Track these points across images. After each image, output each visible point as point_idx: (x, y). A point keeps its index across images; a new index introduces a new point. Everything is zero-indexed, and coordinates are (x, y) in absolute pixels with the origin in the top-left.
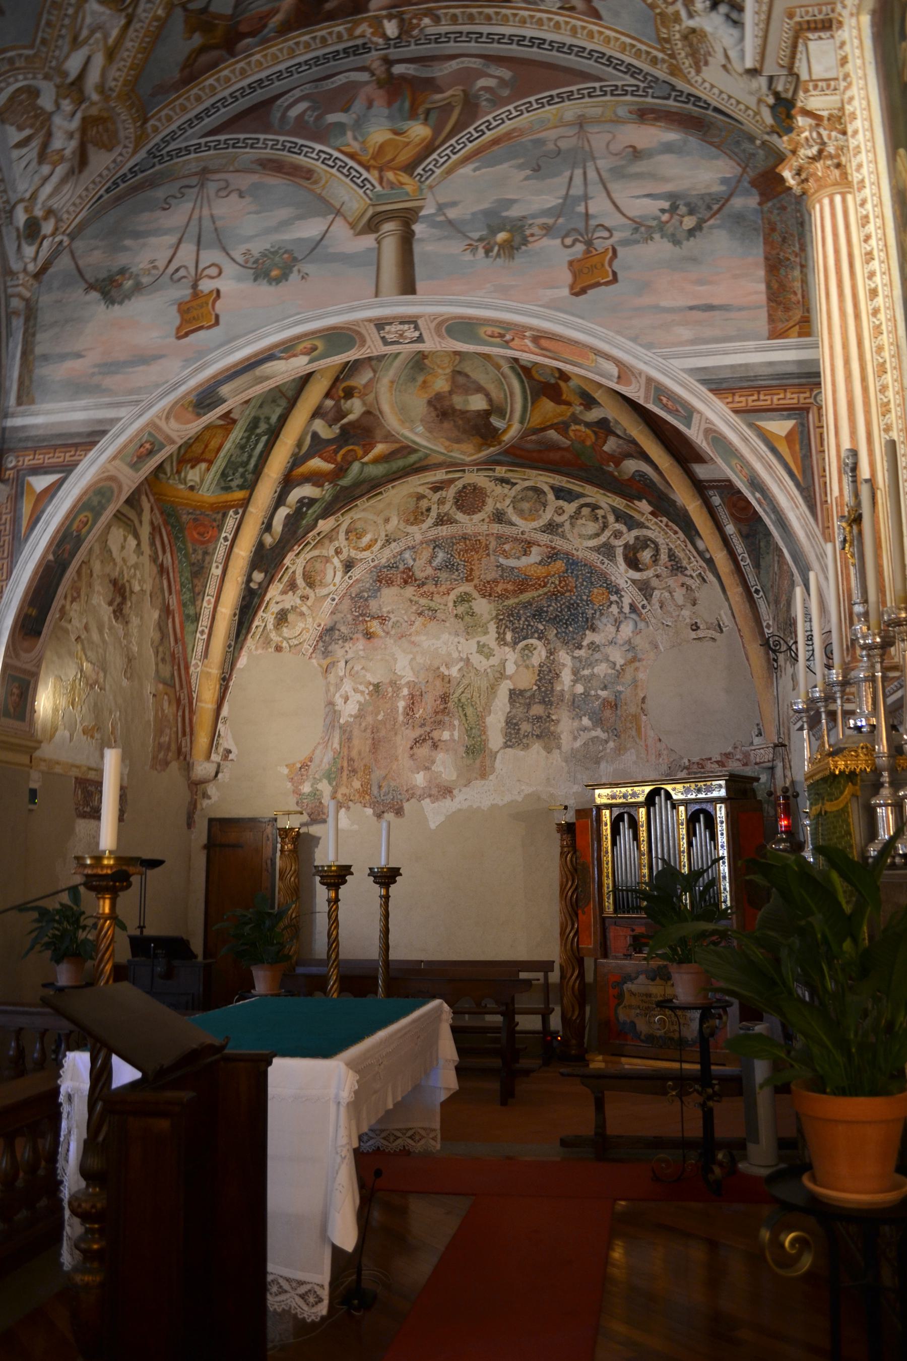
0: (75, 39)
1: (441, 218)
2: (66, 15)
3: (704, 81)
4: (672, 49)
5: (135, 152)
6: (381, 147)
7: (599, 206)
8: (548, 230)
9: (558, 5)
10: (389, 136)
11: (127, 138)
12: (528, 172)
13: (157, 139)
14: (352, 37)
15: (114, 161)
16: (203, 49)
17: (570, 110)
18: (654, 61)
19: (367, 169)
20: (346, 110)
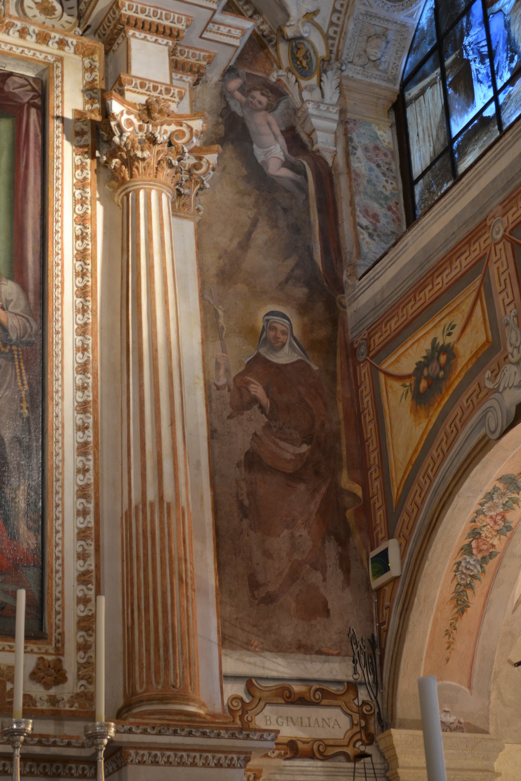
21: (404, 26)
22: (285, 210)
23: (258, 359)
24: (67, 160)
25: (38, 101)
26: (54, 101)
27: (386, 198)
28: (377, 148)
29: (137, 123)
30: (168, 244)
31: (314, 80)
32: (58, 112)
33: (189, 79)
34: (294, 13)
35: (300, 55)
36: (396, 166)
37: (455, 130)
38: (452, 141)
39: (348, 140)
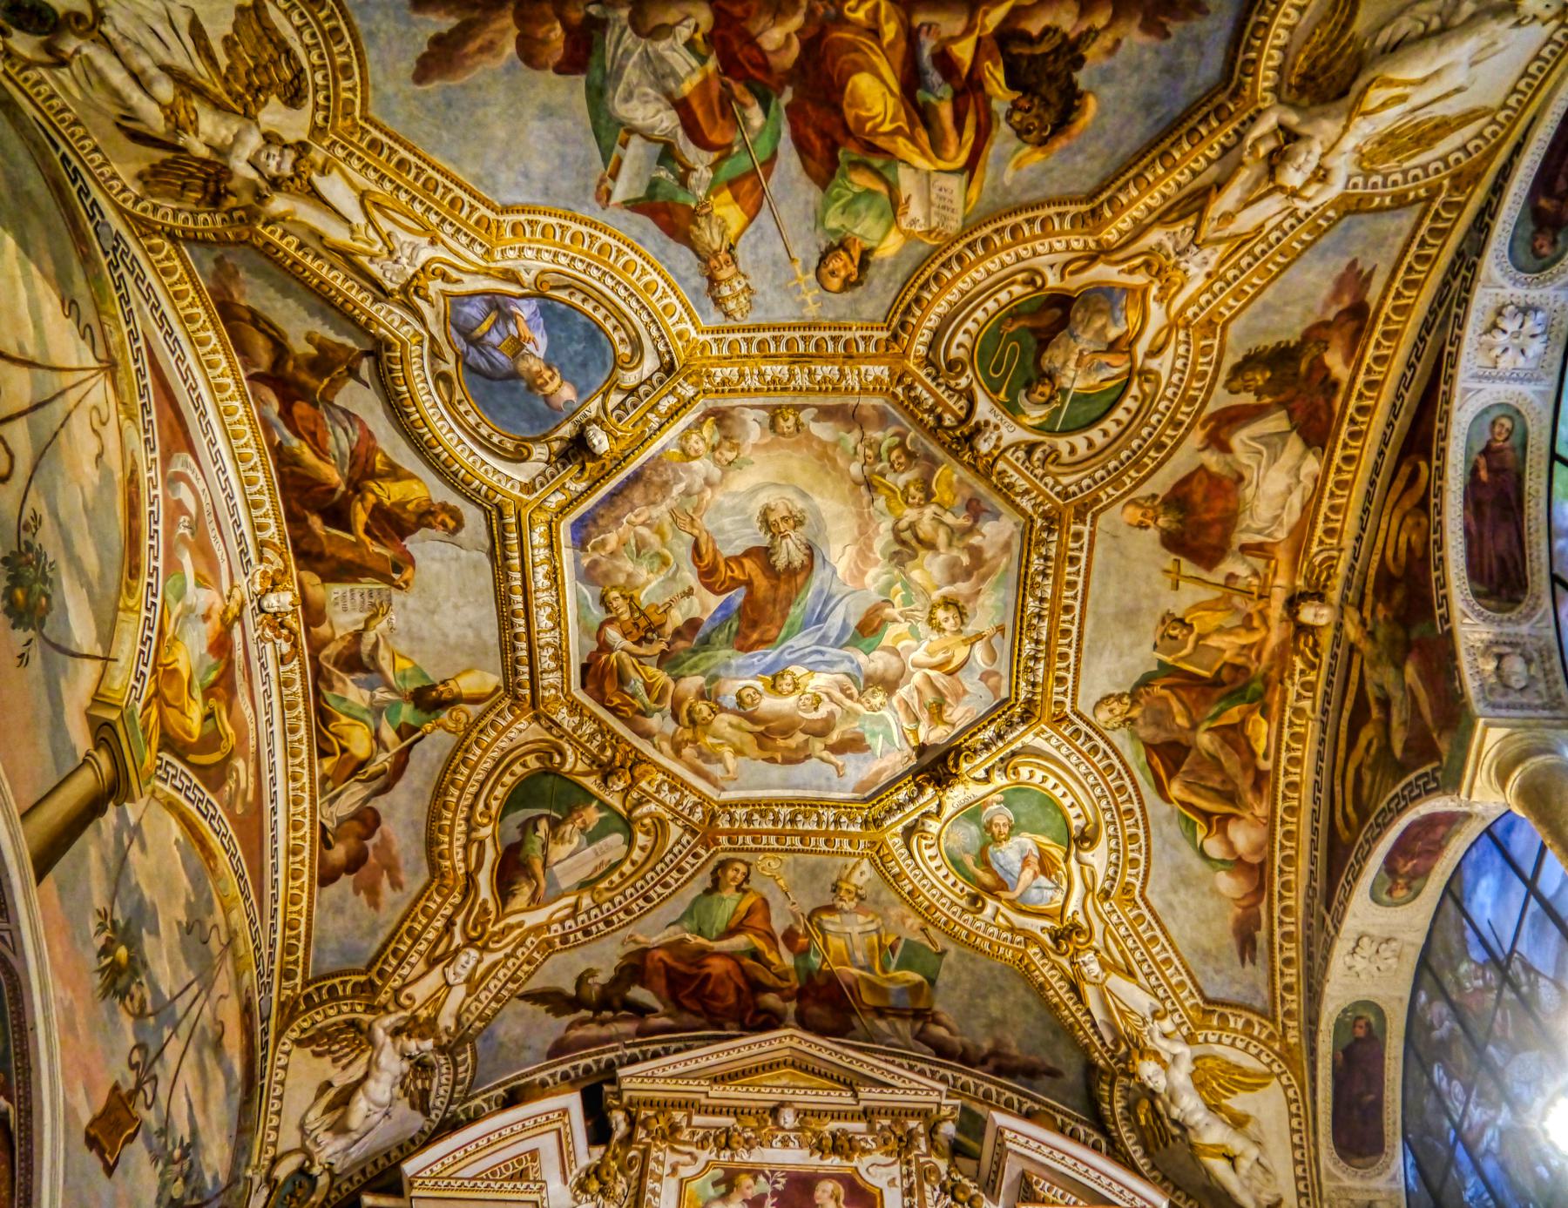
0: (377, 205)
1: (126, 841)
2: (414, 198)
3: (288, 1053)
4: (322, 1003)
5: (121, 211)
6: (175, 671)
7: (172, 1053)
8: (140, 1015)
9: (329, 825)
10: (186, 677)
11: (156, 209)
12: (184, 919)
13: (135, 249)
14: (261, 545)
15: (114, 176)
16: (279, 347)
17: (238, 918)
18: (287, 975)
19: (154, 671)
20: (198, 585)
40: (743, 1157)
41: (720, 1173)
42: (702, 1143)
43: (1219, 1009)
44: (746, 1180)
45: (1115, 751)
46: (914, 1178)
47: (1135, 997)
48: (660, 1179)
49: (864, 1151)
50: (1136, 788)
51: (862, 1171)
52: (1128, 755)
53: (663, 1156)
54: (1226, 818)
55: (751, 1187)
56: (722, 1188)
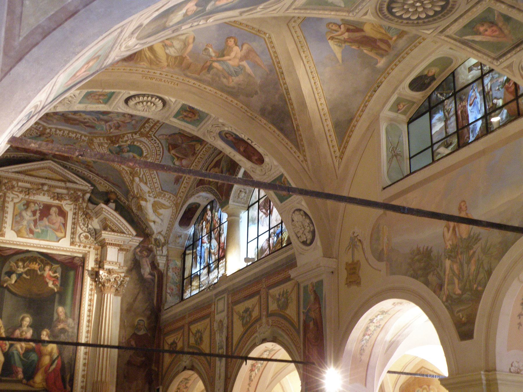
21: (186, 234)
22: (148, 288)
23: (135, 334)
24: (88, 281)
25: (82, 264)
26: (86, 265)
27: (176, 283)
28: (176, 268)
29: (106, 274)
30: (113, 303)
31: (160, 248)
32: (87, 268)
33: (124, 253)
34: (155, 232)
35: (157, 242)
36: (181, 273)
37: (193, 273)
38: (192, 275)
39: (168, 266)
40: (32, 198)
41: (25, 202)
42: (21, 192)
43: (165, 193)
44: (32, 205)
45: (161, 143)
46: (77, 210)
47: (145, 188)
48: (8, 203)
49: (65, 200)
50: (163, 150)
51: (64, 206)
52: (164, 145)
53: (10, 195)
54: (182, 159)
55: (33, 207)
56: (26, 207)
